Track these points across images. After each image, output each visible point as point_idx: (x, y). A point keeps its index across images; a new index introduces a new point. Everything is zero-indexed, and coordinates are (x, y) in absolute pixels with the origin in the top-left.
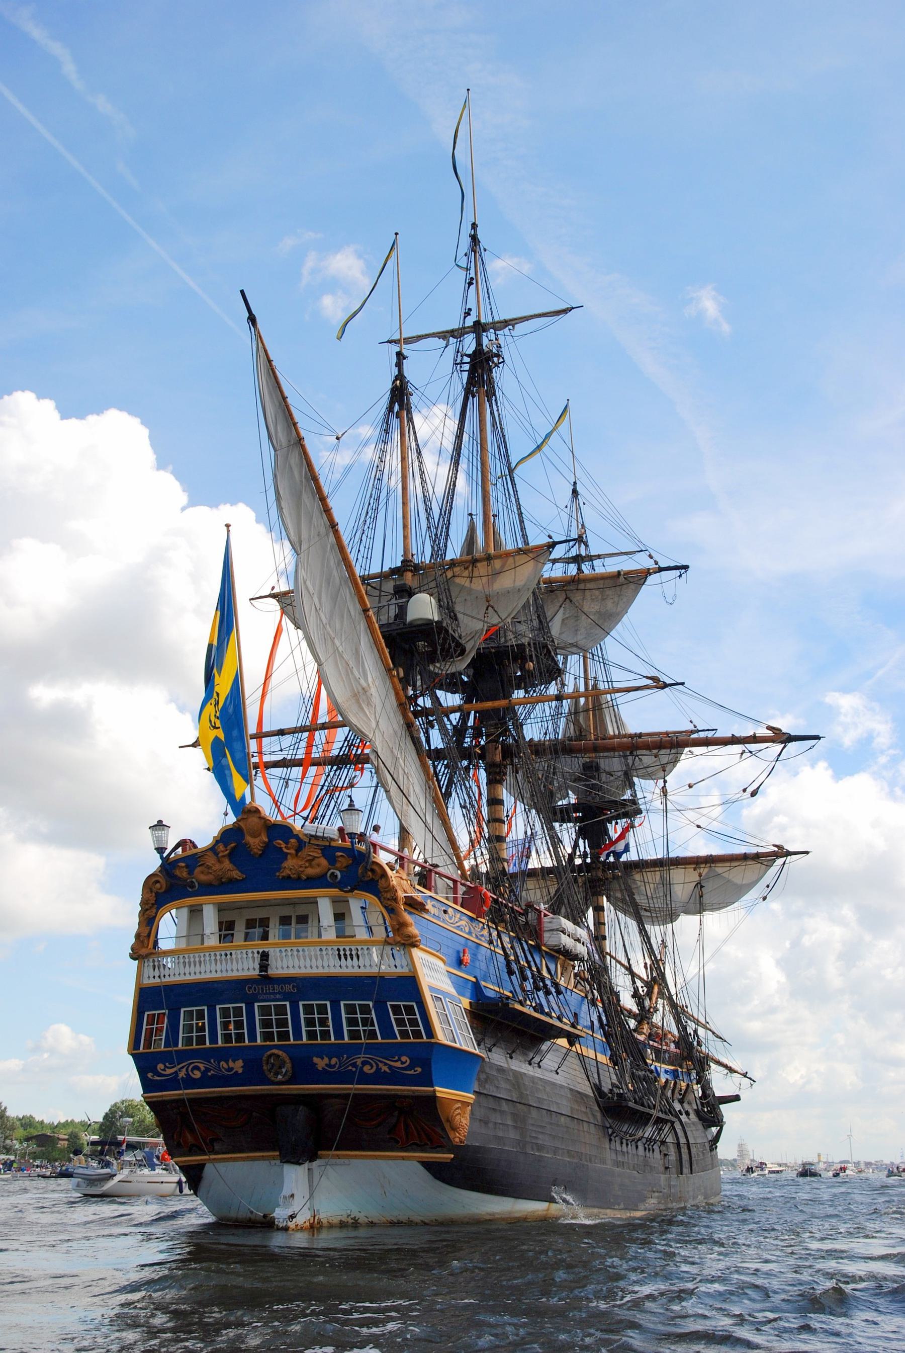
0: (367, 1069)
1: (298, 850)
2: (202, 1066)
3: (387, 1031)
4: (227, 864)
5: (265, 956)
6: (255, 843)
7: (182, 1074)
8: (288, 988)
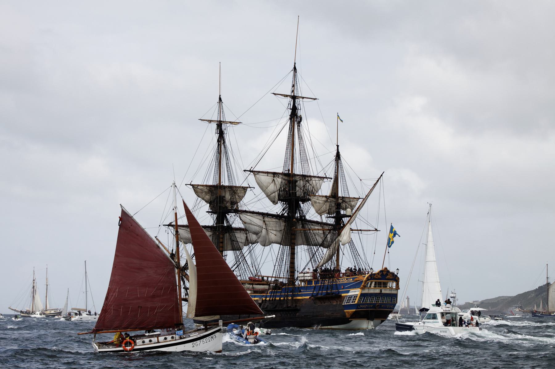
0: (388, 307)
1: (390, 274)
2: (367, 306)
3: (391, 302)
4: (380, 276)
5: (381, 290)
6: (385, 273)
7: (363, 307)
8: (382, 295)
